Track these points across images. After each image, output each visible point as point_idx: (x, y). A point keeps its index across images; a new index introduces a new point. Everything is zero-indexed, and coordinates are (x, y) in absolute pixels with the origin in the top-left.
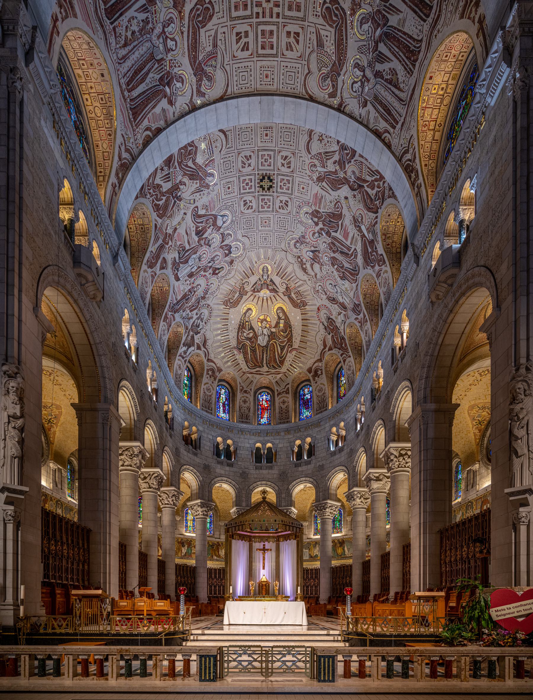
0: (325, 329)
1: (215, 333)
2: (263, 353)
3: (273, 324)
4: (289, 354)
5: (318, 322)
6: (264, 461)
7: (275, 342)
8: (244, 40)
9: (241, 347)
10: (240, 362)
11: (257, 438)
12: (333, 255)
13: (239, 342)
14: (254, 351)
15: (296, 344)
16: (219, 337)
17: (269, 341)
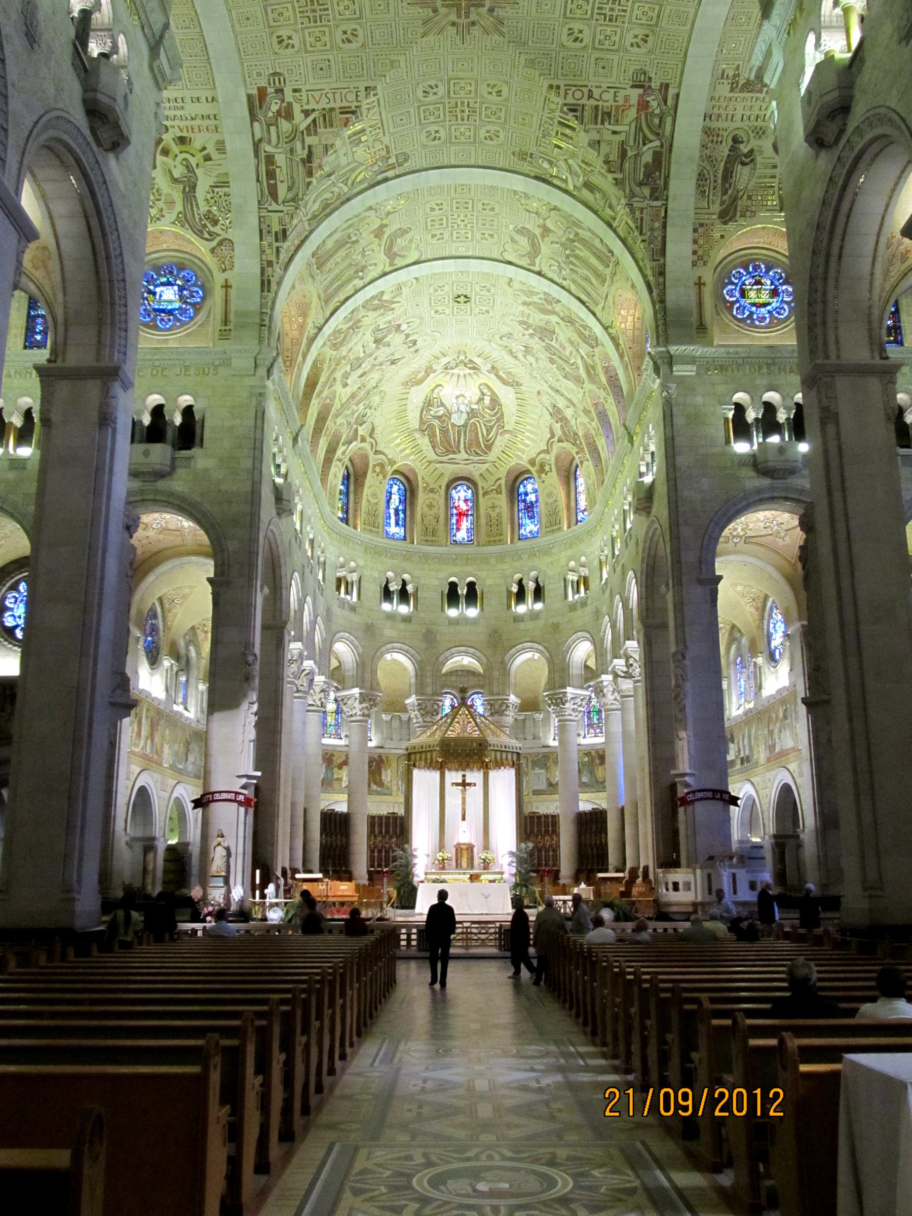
0: (551, 415)
2: (459, 434)
3: (476, 399)
4: (499, 437)
5: (540, 406)
8: (437, 208)
9: (425, 428)
10: (424, 448)
13: (422, 421)
14: (445, 432)
16: (393, 421)
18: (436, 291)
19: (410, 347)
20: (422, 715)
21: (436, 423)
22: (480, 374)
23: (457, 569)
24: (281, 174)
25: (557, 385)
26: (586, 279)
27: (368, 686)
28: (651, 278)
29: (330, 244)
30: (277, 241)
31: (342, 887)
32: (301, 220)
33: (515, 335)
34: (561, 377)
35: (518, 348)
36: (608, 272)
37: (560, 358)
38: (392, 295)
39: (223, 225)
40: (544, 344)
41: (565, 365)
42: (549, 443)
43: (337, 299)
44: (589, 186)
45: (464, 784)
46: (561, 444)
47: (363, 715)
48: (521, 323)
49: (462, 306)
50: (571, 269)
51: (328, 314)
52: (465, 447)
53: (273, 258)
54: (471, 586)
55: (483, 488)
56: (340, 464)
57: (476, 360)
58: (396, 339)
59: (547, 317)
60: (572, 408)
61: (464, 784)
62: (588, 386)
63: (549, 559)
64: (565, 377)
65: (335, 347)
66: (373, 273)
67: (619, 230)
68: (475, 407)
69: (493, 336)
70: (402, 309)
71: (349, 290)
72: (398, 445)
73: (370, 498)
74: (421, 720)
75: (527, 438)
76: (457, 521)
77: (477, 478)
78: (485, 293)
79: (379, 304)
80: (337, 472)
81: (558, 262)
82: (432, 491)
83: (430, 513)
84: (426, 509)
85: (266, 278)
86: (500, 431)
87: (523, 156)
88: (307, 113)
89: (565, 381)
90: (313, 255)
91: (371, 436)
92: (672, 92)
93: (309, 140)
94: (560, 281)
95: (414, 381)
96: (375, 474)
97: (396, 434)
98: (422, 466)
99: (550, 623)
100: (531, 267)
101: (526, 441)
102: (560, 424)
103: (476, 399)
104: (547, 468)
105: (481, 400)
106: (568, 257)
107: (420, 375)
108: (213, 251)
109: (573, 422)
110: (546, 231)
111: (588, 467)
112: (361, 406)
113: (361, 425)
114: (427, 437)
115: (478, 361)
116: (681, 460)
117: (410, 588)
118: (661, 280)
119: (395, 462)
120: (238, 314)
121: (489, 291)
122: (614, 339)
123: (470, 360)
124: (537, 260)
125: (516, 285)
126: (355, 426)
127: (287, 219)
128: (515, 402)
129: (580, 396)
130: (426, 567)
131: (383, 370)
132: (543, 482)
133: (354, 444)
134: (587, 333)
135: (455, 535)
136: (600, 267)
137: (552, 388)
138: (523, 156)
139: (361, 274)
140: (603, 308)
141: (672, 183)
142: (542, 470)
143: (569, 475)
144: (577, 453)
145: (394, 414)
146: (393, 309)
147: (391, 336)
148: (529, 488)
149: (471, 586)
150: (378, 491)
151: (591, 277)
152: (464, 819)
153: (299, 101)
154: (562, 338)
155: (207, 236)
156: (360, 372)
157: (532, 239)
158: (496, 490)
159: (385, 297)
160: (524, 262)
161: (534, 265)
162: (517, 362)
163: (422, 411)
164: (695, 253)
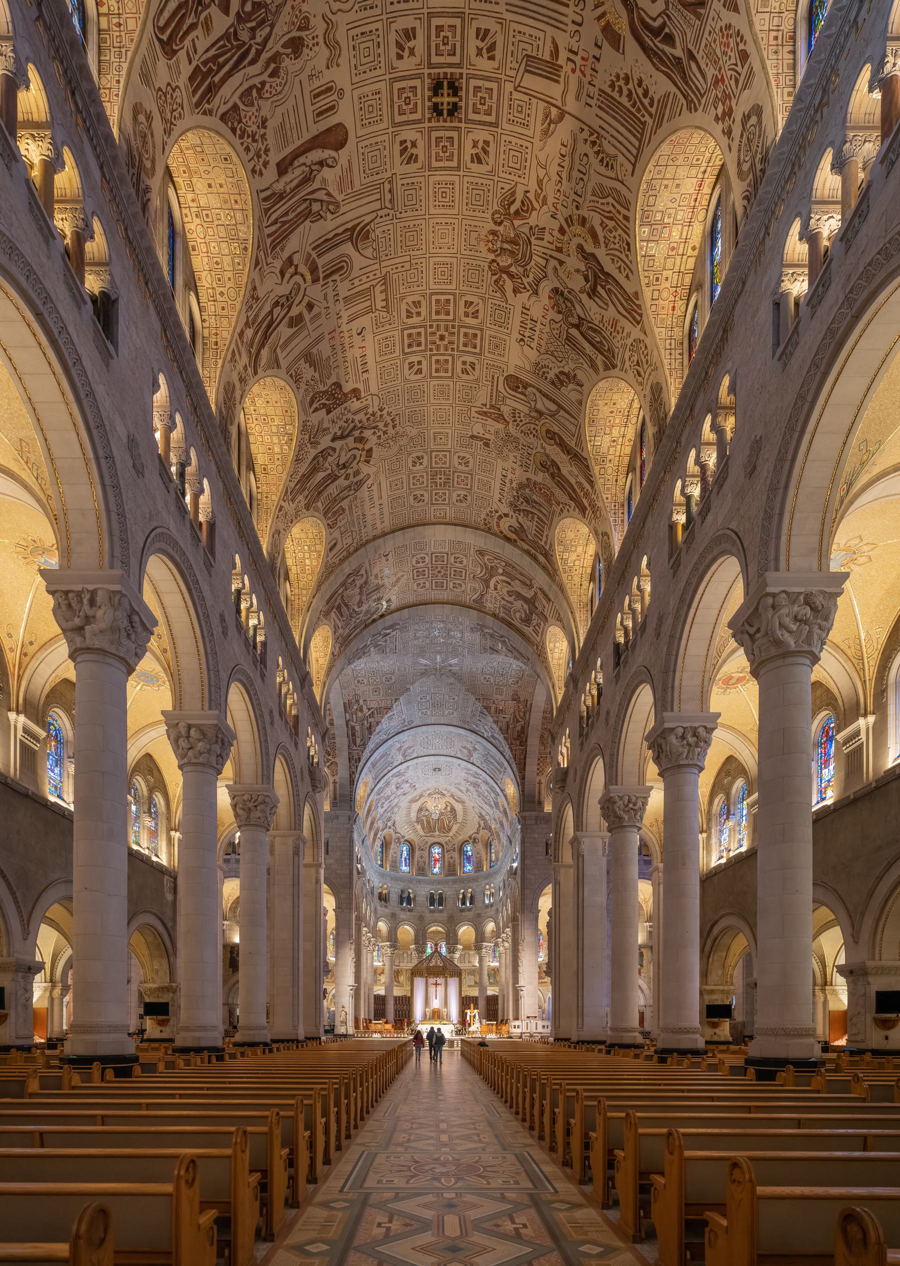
6: (436, 897)
9: (419, 820)
11: (431, 887)
14: (428, 822)
15: (460, 818)
21: (424, 819)
24: (358, 734)
42: (478, 830)
44: (492, 736)
58: (406, 786)
65: (378, 794)
71: (386, 771)
77: (443, 842)
79: (399, 774)
87: (465, 722)
88: (369, 709)
92: (529, 703)
93: (370, 720)
95: (414, 801)
105: (446, 808)
110: (475, 749)
115: (445, 792)
122: (505, 796)
138: (465, 722)
141: (529, 739)
143: (488, 845)
148: (469, 848)
153: (366, 705)
157: (469, 751)
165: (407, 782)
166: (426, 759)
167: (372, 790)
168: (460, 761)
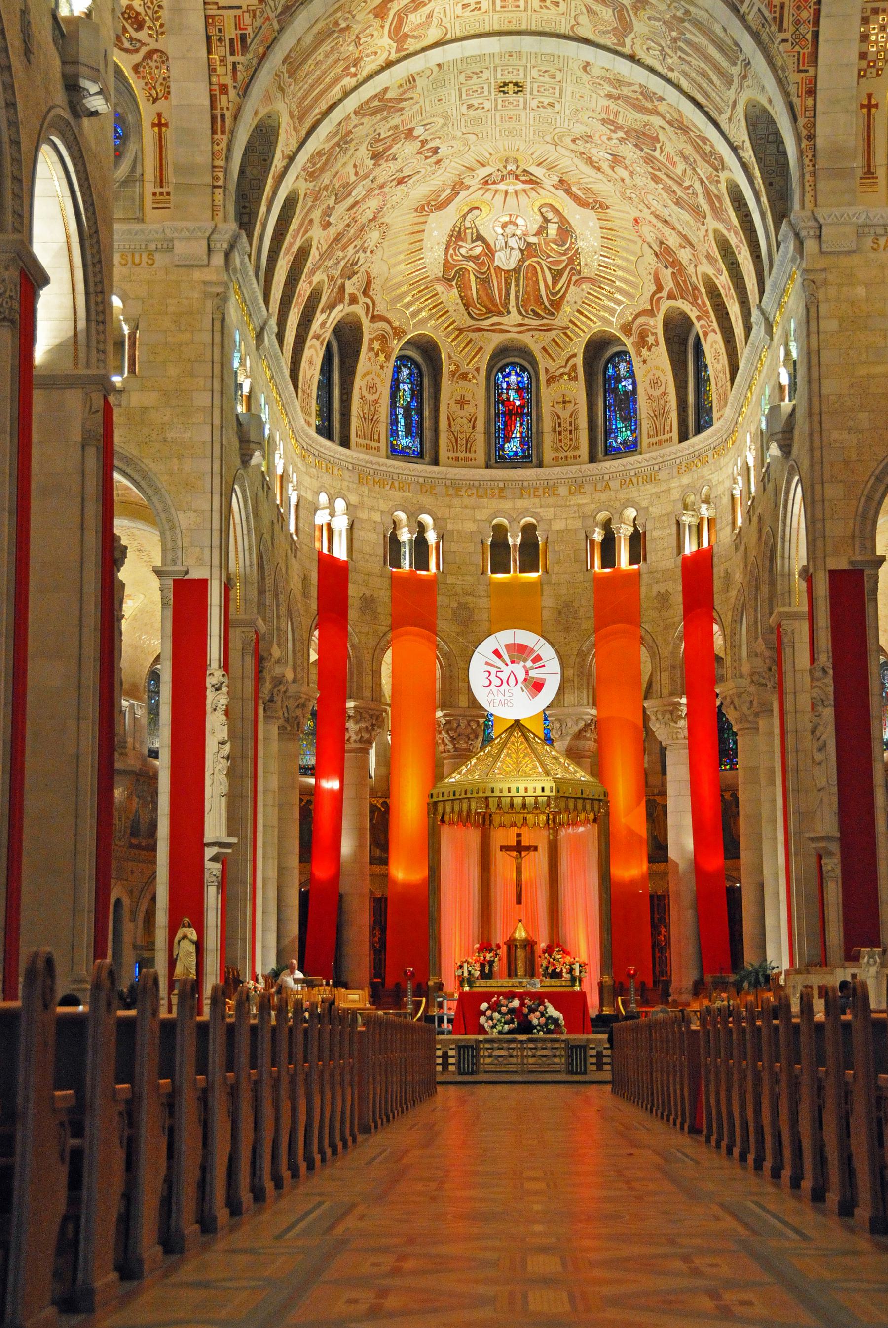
0: (656, 255)
1: (392, 261)
4: (572, 288)
5: (640, 242)
7: (538, 263)
12: (651, 170)
14: (484, 282)
16: (402, 267)
17: (522, 261)
18: (468, 78)
19: (427, 158)
20: (453, 739)
22: (541, 191)
23: (507, 505)
25: (665, 213)
26: (704, 74)
27: (367, 694)
28: (796, 100)
29: (308, 40)
30: (232, 53)
31: (351, 997)
32: (268, 19)
33: (596, 137)
34: (670, 202)
35: (601, 155)
36: (735, 70)
37: (668, 176)
38: (401, 90)
39: (150, 28)
40: (643, 154)
41: (675, 187)
42: (654, 299)
43: (317, 111)
45: (519, 848)
46: (672, 303)
47: (361, 741)
48: (604, 122)
49: (511, 97)
50: (680, 57)
51: (303, 133)
52: (517, 305)
53: (228, 80)
54: (529, 531)
55: (547, 370)
56: (315, 342)
57: (533, 169)
59: (646, 118)
60: (689, 249)
61: (519, 848)
62: (712, 223)
63: (651, 489)
64: (677, 203)
66: (369, 65)
67: (750, 18)
68: (533, 240)
69: (560, 138)
70: (417, 107)
71: (335, 93)
72: (408, 305)
73: (365, 393)
74: (450, 746)
75: (620, 290)
76: (505, 424)
78: (546, 79)
80: (314, 353)
81: (660, 45)
82: (464, 376)
83: (462, 413)
84: (455, 407)
85: (218, 112)
86: (574, 279)
89: (676, 209)
90: (284, 62)
91: (365, 293)
94: (664, 71)
96: (372, 354)
97: (404, 288)
98: (447, 336)
99: (654, 593)
100: (619, 48)
101: (618, 296)
102: (670, 270)
103: (536, 227)
104: (651, 339)
105: (541, 231)
106: (675, 40)
107: (444, 195)
108: (136, 68)
109: (691, 269)
111: (716, 342)
112: (351, 250)
113: (349, 278)
114: (455, 290)
115: (539, 172)
116: (830, 387)
117: (431, 537)
118: (810, 102)
119: (404, 333)
120: (180, 169)
121: (553, 77)
123: (525, 171)
124: (628, 40)
125: (596, 71)
126: (340, 282)
127: (247, 19)
128: (599, 233)
129: (701, 234)
130: (456, 502)
131: (385, 195)
132: (645, 362)
133: (339, 308)
134: (708, 149)
135: (502, 448)
136: (724, 63)
137: (657, 217)
139: (353, 70)
140: (730, 119)
142: (642, 341)
144: (699, 318)
145: (402, 257)
146: (402, 109)
147: (399, 145)
149: (529, 531)
150: (377, 380)
151: (710, 73)
152: (519, 901)
154: (668, 148)
155: (127, 45)
156: (350, 201)
158: (569, 374)
159: (389, 95)
160: (609, 40)
161: (624, 45)
162: (600, 176)
163: (447, 249)
164: (863, 56)
165: (409, 134)
166: (472, 47)
167: (291, 159)
168: (587, 53)
